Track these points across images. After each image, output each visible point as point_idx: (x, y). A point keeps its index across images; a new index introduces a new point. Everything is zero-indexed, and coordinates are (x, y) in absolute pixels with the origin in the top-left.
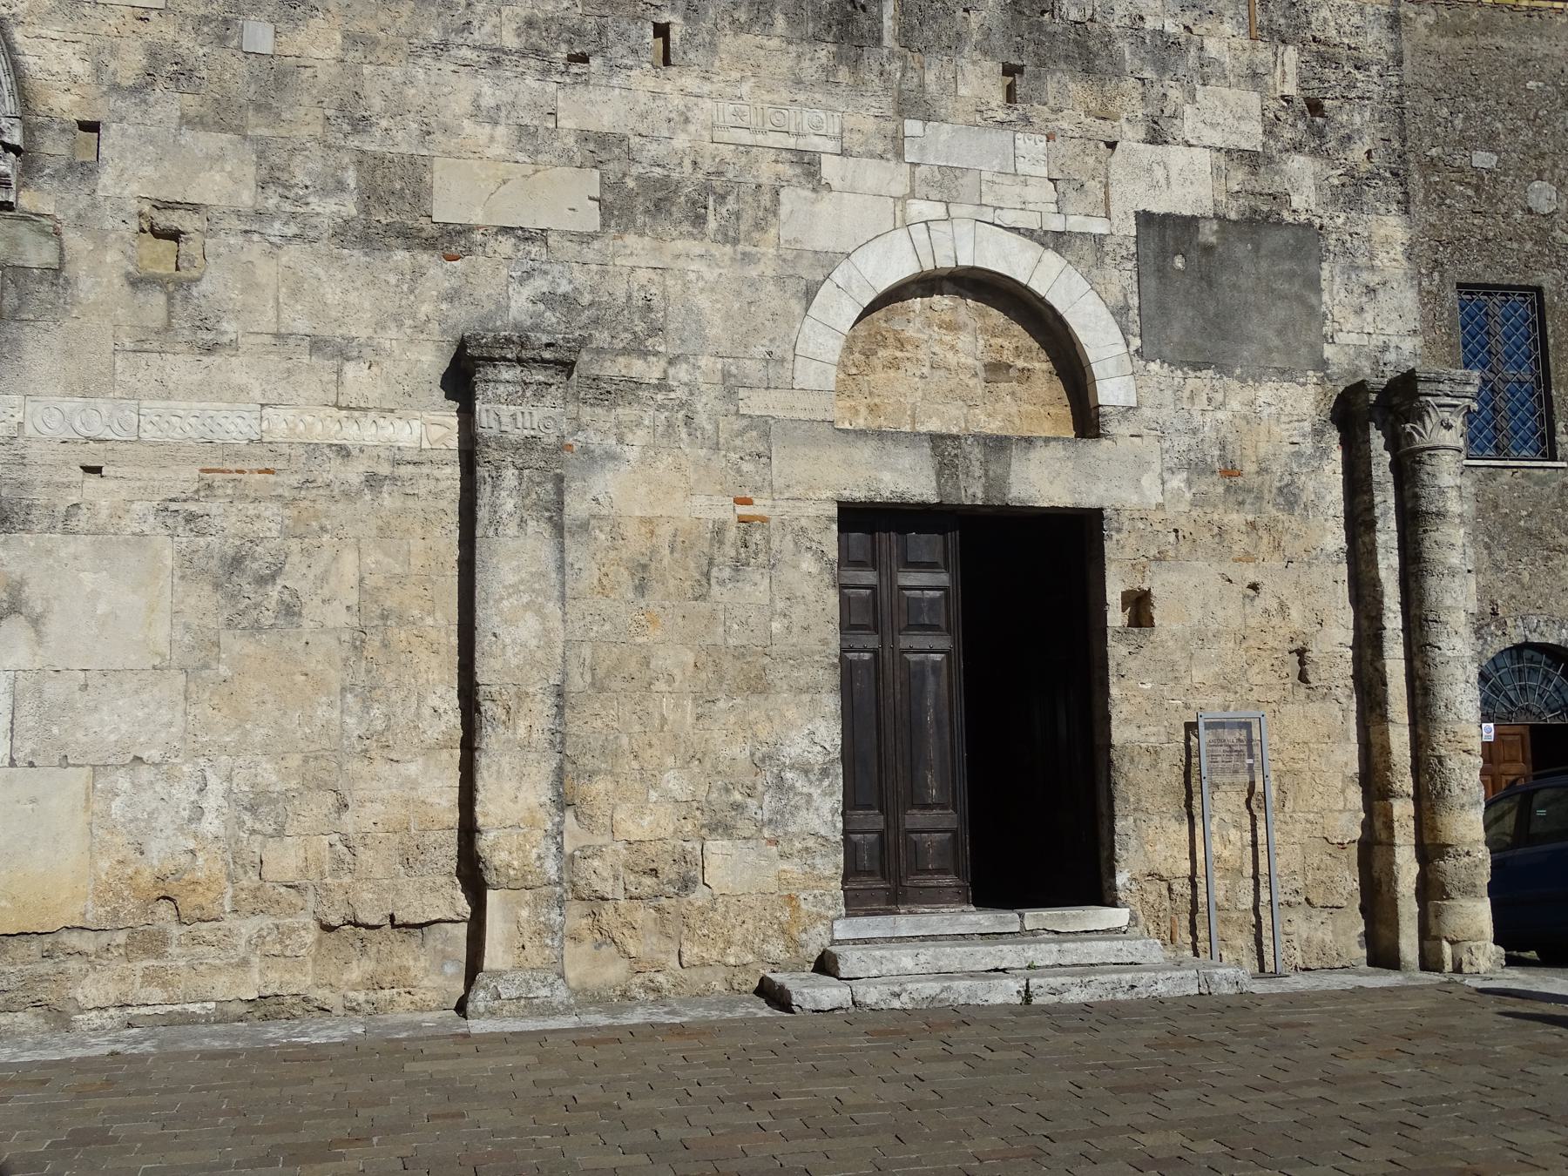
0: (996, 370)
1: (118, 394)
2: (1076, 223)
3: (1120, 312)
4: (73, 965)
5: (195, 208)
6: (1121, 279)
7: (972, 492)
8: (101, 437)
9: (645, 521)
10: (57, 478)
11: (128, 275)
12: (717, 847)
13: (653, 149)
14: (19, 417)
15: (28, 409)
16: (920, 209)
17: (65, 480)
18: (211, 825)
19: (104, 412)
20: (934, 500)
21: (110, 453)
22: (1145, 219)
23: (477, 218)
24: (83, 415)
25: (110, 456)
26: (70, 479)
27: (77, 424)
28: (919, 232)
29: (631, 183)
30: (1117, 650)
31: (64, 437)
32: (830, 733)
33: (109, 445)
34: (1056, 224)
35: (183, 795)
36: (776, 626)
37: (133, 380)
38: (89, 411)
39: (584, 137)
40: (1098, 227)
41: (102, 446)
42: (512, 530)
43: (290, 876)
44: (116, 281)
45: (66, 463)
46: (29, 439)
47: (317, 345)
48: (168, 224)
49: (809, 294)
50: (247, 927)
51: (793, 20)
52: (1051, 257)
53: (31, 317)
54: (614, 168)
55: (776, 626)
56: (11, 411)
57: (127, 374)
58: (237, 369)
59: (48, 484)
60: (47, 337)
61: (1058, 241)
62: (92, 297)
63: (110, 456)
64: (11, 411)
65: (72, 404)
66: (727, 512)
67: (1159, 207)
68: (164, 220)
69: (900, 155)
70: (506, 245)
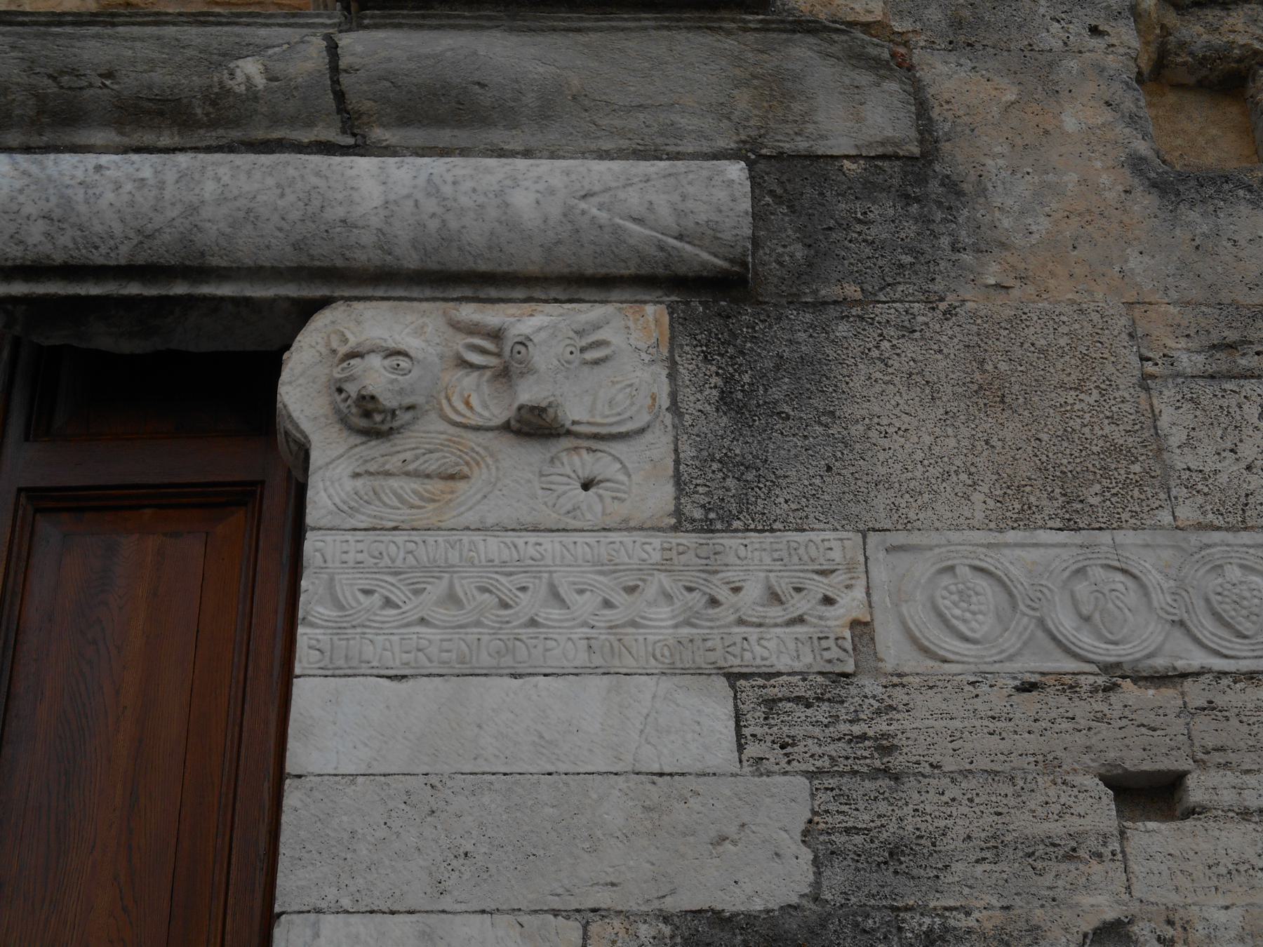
1: (1186, 513)
8: (1160, 663)
10: (1023, 824)
11: (1137, 164)
14: (851, 604)
15: (880, 574)
17: (1055, 828)
19: (1153, 578)
21: (1202, 724)
24: (1082, 588)
25: (1206, 731)
26: (1074, 824)
27: (1066, 623)
31: (1029, 665)
33: (1196, 693)
37: (1230, 467)
38: (1097, 573)
41: (1168, 696)
44: (1105, 179)
45: (1049, 764)
46: (898, 679)
48: (1216, 40)
53: (852, 291)
56: (821, 586)
57: (1206, 448)
59: (995, 847)
60: (910, 348)
62: (1041, 226)
63: (1206, 731)
64: (821, 586)
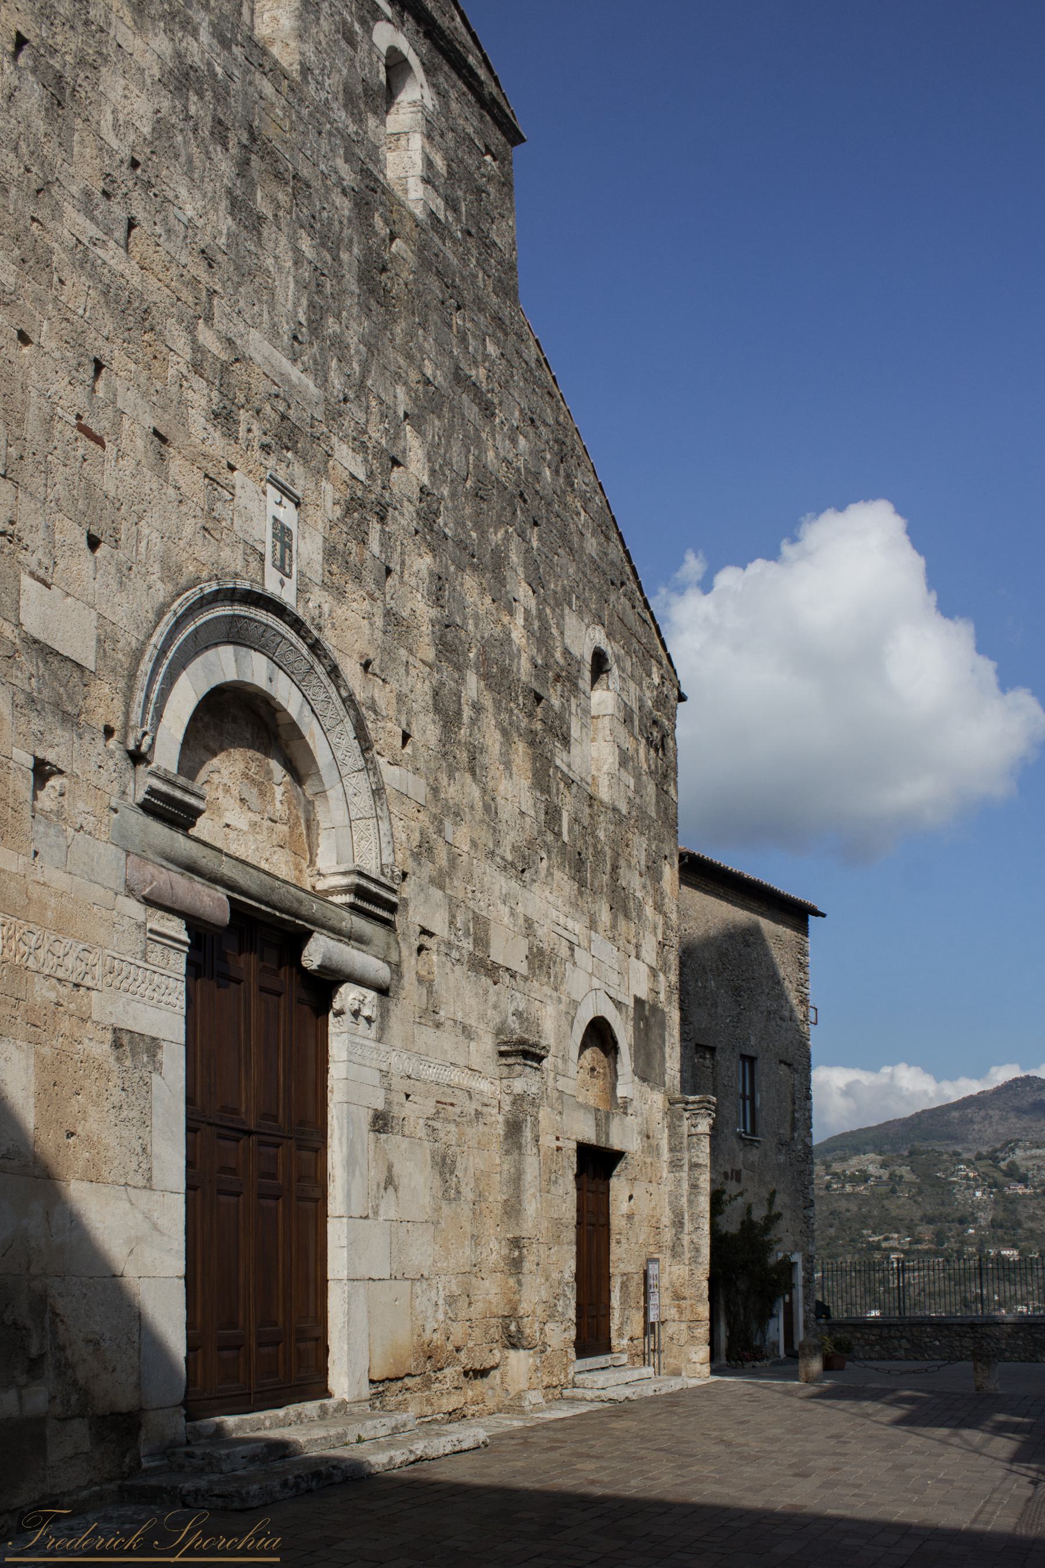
23: (501, 962)
70: (506, 977)
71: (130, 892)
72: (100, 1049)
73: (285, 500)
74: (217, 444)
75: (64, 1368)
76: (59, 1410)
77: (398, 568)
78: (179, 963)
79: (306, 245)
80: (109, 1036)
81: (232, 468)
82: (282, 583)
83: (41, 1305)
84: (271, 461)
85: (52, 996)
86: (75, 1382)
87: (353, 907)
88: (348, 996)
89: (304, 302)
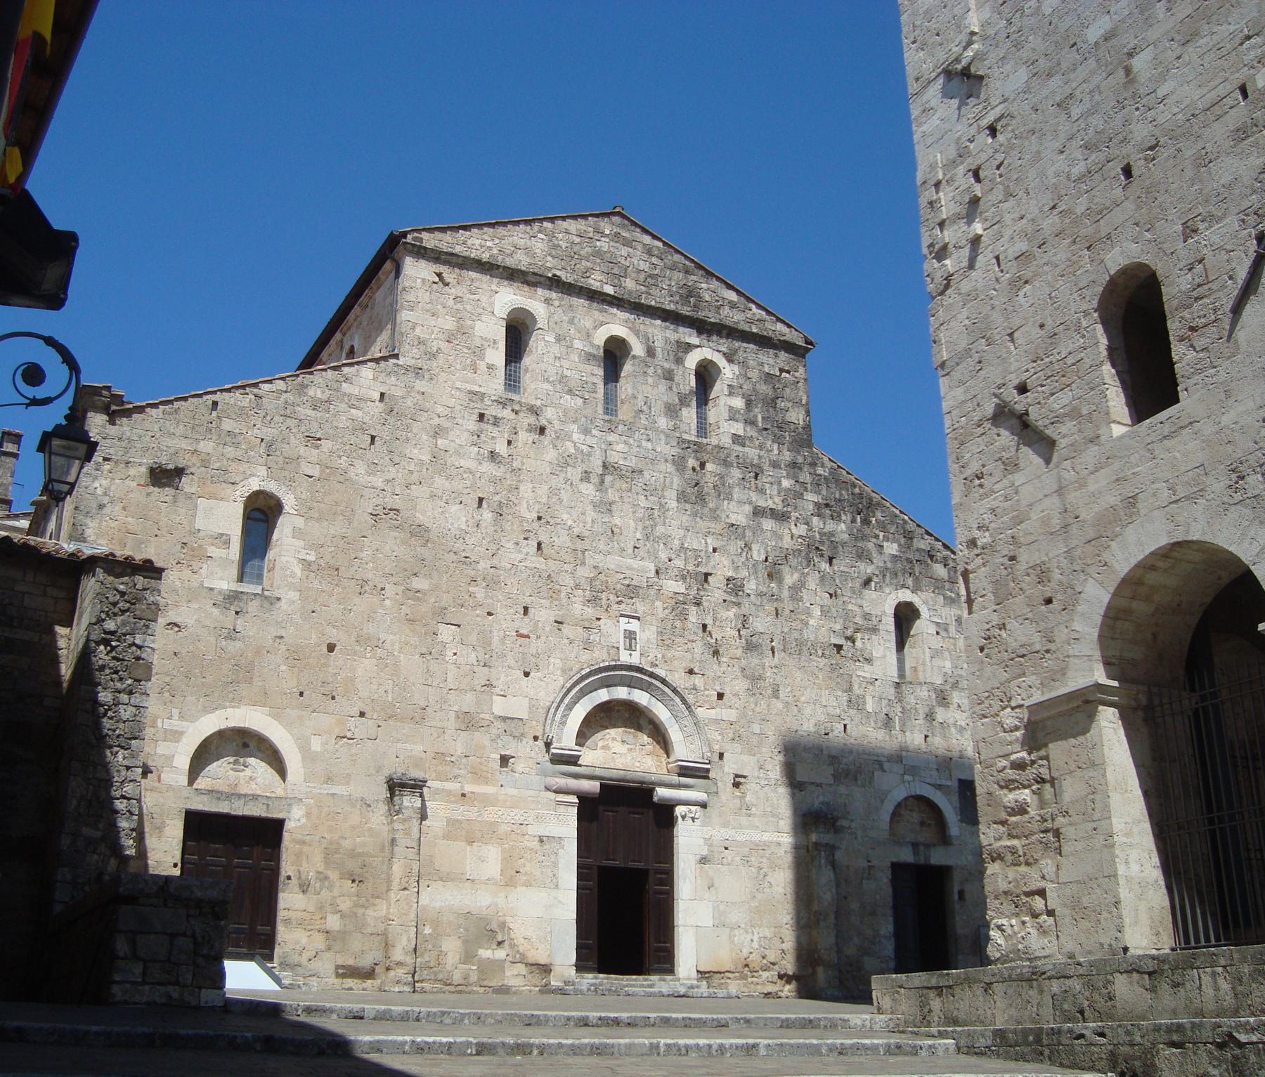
0: (922, 823)
2: (943, 782)
3: (955, 808)
4: (729, 981)
5: (745, 777)
6: (955, 798)
7: (922, 861)
9: (848, 867)
12: (866, 958)
13: (845, 760)
16: (907, 778)
18: (755, 945)
20: (913, 862)
22: (960, 780)
23: (806, 779)
28: (907, 785)
29: (840, 770)
30: (957, 906)
32: (891, 928)
34: (939, 782)
35: (749, 937)
36: (878, 897)
39: (829, 756)
40: (949, 783)
42: (824, 868)
43: (772, 961)
47: (773, 815)
49: (882, 802)
50: (765, 975)
51: (876, 722)
52: (937, 791)
54: (836, 766)
55: (878, 897)
58: (756, 821)
61: (939, 787)
65: (723, 830)
66: (865, 864)
67: (963, 778)
68: (737, 779)
69: (902, 762)
71: (547, 789)
72: (535, 844)
73: (631, 620)
74: (590, 612)
75: (512, 946)
76: (511, 959)
77: (711, 622)
78: (575, 810)
79: (643, 502)
80: (537, 839)
81: (599, 619)
82: (631, 655)
83: (503, 925)
84: (623, 606)
85: (510, 829)
86: (518, 951)
87: (680, 775)
88: (679, 810)
89: (640, 528)
